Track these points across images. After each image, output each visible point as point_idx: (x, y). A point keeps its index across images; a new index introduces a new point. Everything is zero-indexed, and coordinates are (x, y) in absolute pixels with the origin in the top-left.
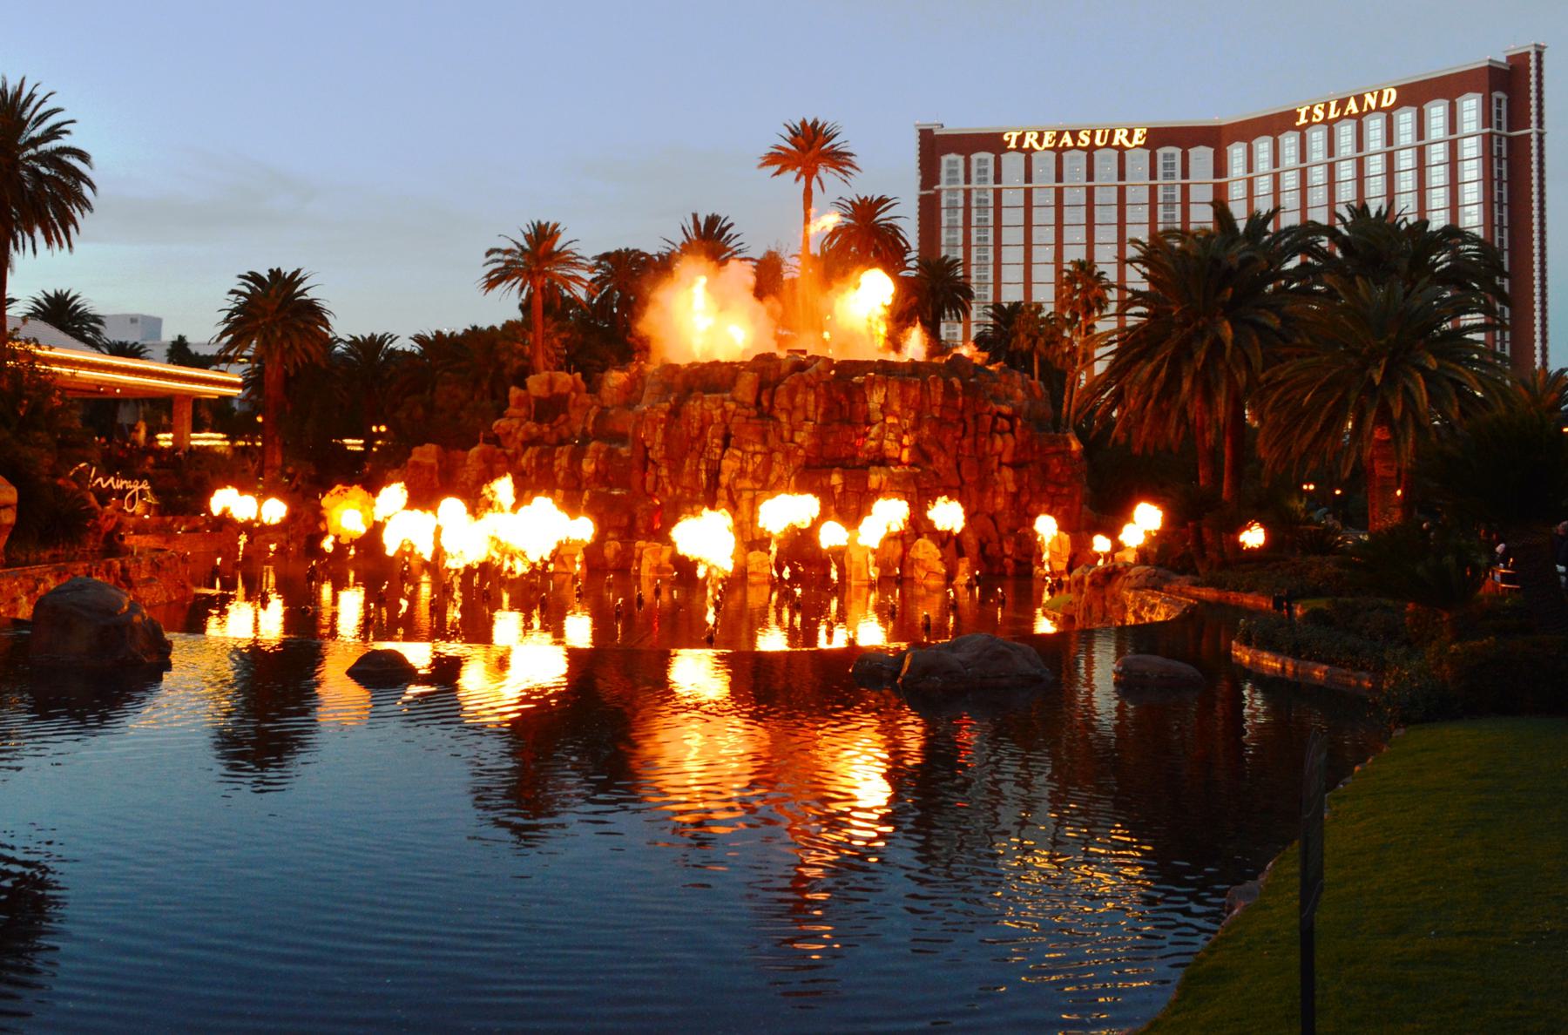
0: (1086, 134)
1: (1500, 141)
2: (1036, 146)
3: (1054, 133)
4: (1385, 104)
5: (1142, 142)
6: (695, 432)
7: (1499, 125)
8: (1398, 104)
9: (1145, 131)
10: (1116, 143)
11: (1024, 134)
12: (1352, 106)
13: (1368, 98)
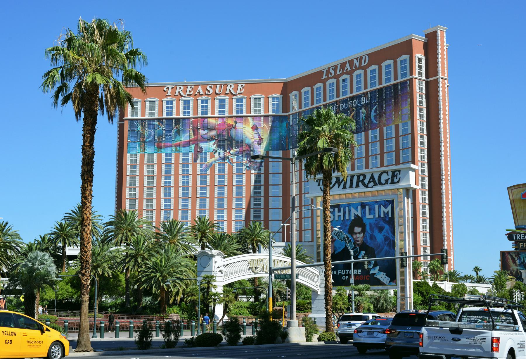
0: (211, 87)
2: (182, 93)
4: (363, 64)
8: (369, 65)
12: (348, 67)
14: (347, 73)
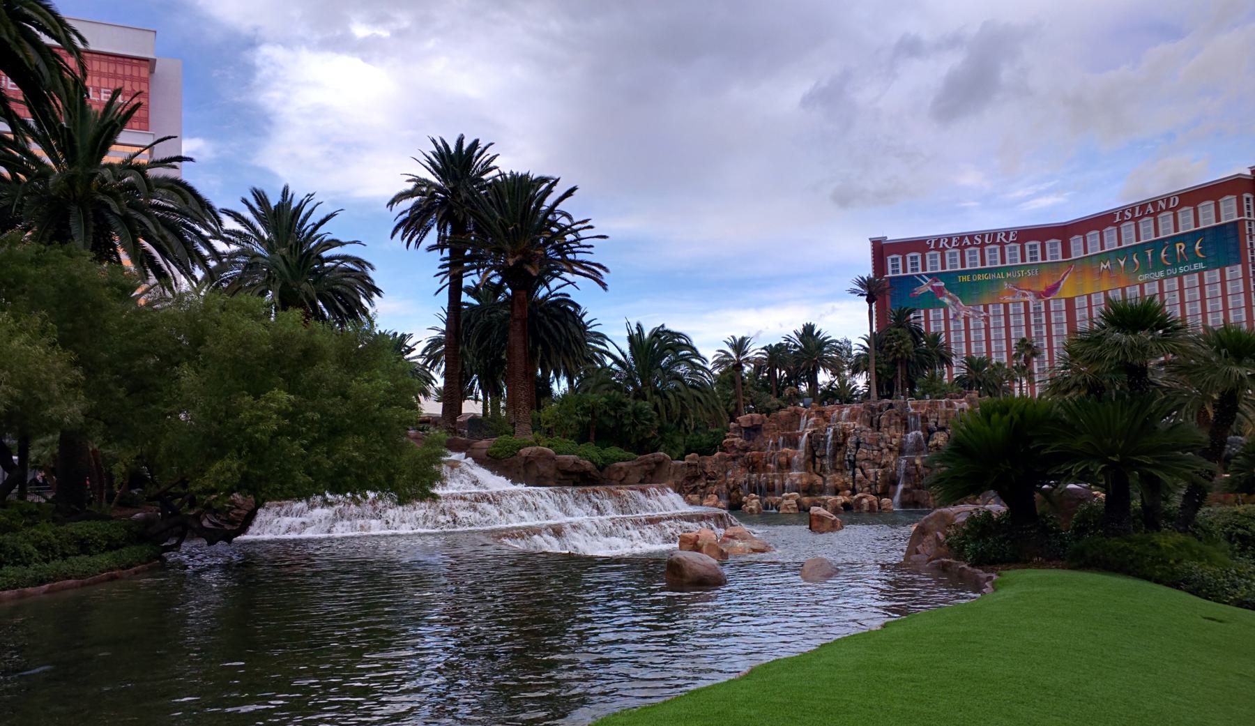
1: (1250, 224)
2: (947, 246)
4: (1171, 206)
6: (841, 441)
7: (1249, 214)
8: (1180, 206)
10: (998, 241)
11: (939, 240)
12: (1150, 209)
13: (1160, 202)
14: (1149, 215)
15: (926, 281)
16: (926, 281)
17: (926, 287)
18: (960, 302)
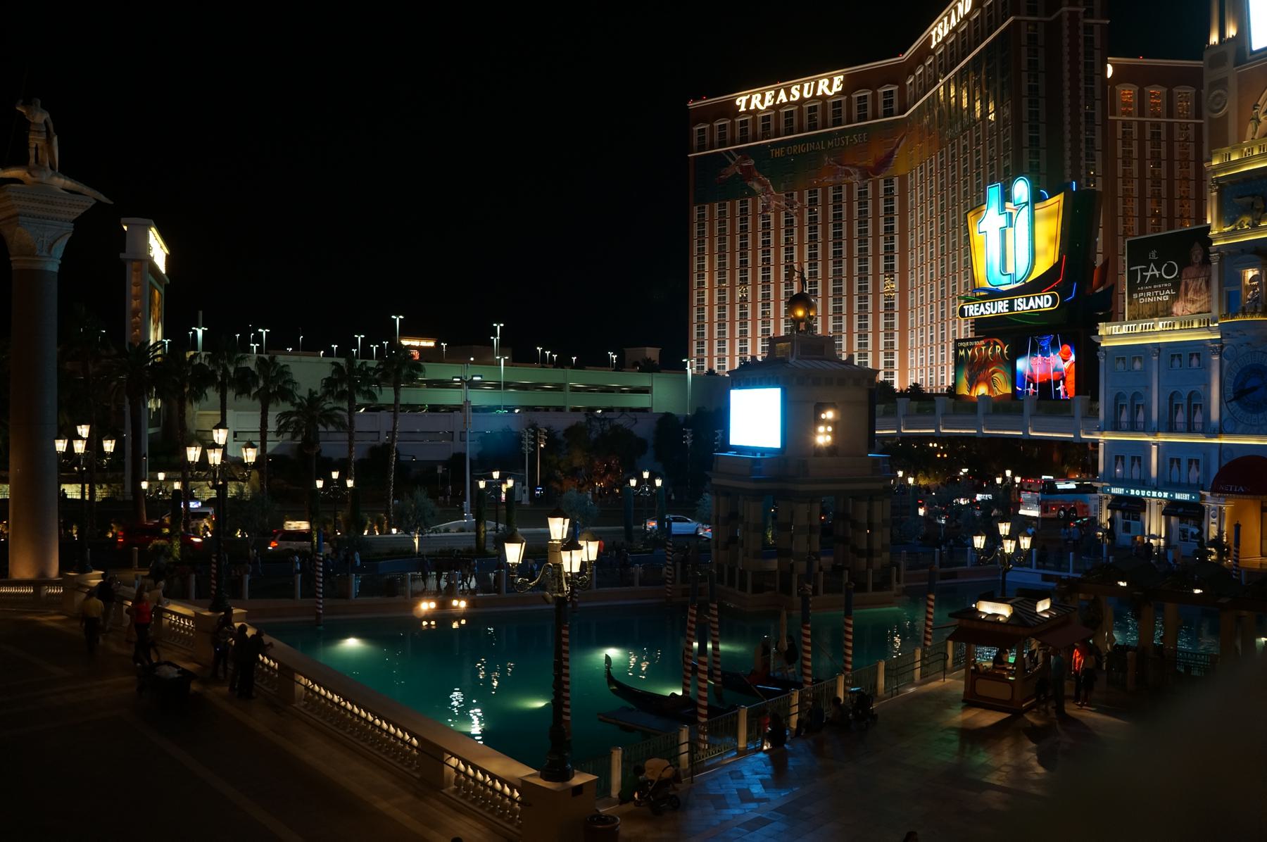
2: (760, 107)
3: (773, 92)
5: (840, 89)
9: (842, 77)
15: (734, 159)
16: (734, 159)
17: (734, 169)
18: (771, 188)
